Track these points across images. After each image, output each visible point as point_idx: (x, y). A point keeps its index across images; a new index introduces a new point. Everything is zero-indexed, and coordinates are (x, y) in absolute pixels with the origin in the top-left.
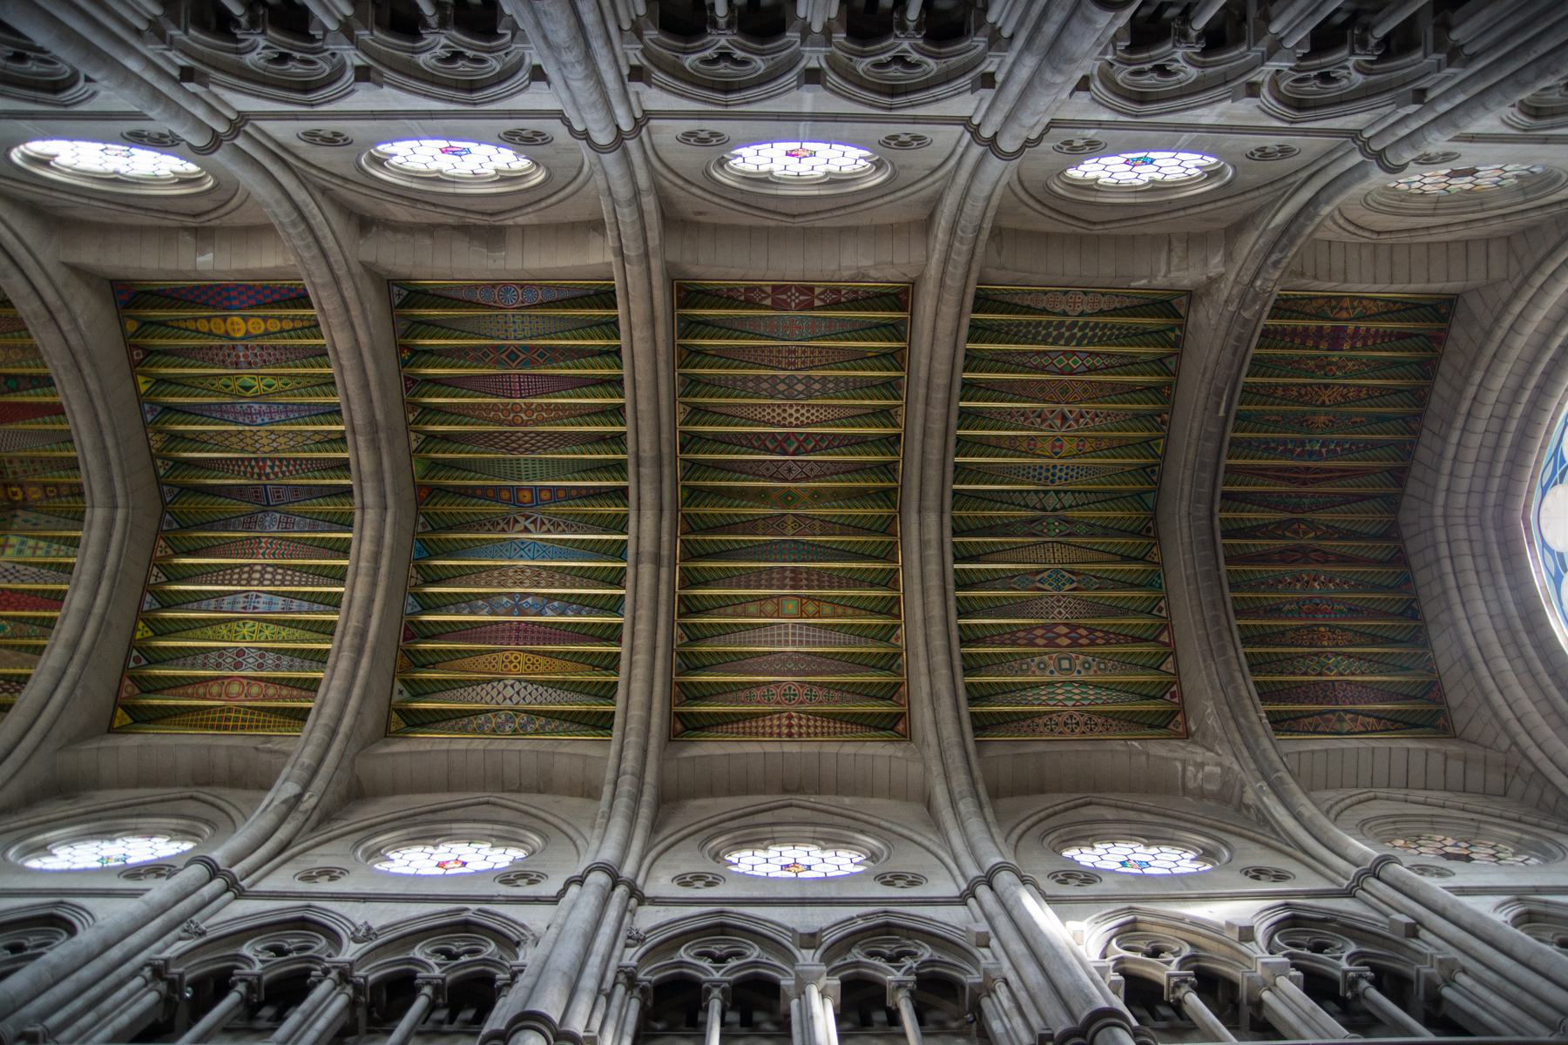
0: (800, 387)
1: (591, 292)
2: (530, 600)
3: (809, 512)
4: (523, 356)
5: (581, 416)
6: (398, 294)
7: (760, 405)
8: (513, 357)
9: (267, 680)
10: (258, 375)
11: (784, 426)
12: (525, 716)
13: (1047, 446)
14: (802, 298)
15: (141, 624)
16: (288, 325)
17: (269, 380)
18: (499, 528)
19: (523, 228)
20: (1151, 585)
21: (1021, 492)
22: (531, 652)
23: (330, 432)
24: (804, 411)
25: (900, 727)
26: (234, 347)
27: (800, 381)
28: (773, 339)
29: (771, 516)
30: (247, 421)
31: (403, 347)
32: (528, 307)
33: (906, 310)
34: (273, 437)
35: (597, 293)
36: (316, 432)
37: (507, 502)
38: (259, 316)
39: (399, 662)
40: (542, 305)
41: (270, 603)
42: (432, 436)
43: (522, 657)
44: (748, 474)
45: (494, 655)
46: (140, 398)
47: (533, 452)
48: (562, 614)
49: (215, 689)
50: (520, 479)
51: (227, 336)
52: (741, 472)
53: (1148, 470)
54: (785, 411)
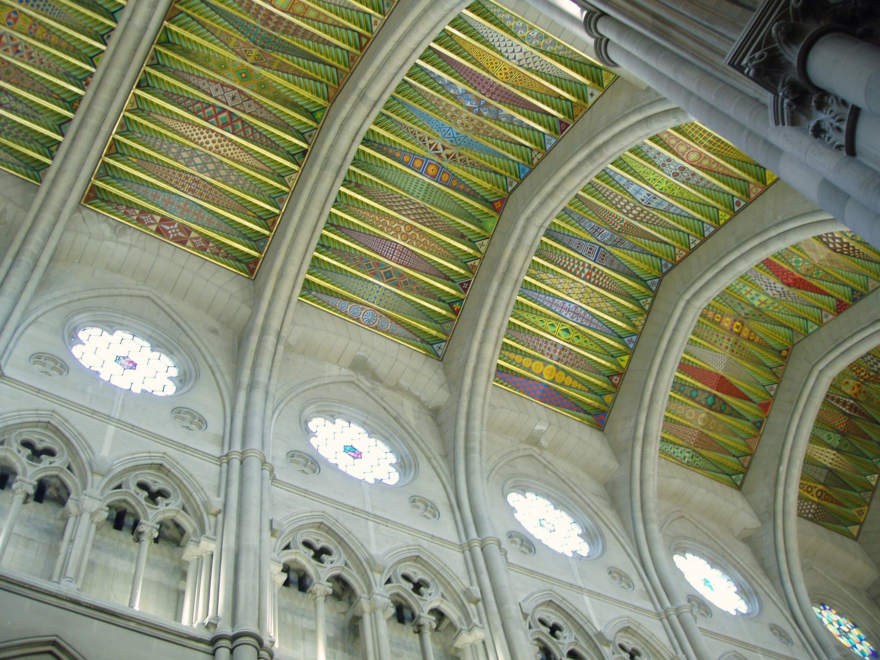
0: (198, 160)
2: (468, 104)
3: (233, 57)
4: (382, 272)
6: (440, 348)
7: (233, 160)
8: (388, 274)
9: (670, 150)
11: (222, 135)
12: (520, 33)
13: (20, 22)
14: (167, 228)
15: (722, 222)
16: (518, 358)
17: (551, 329)
22: (488, 72)
24: (203, 140)
26: (558, 360)
27: (196, 165)
28: (201, 206)
29: (264, 67)
30: (579, 309)
31: (456, 313)
32: (361, 304)
33: (93, 185)
34: (570, 291)
37: (446, 171)
38: (532, 373)
39: (580, 114)
40: (351, 301)
41: (637, 192)
42: (471, 243)
44: (266, 109)
46: (631, 353)
47: (410, 200)
49: (705, 162)
50: (429, 184)
52: (270, 112)
54: (217, 147)
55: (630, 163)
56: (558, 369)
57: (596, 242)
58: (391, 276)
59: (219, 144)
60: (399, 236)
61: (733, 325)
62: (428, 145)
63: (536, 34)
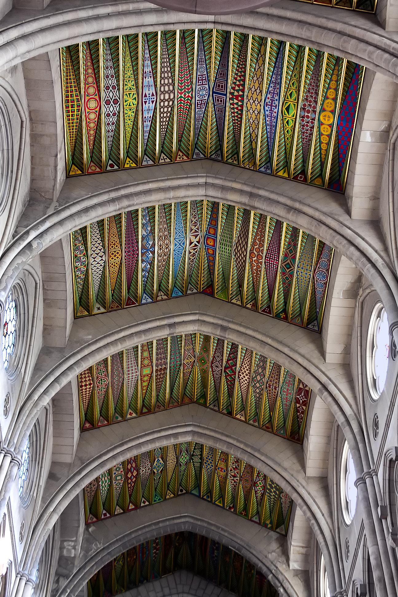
1: (318, 310)
2: (151, 255)
5: (253, 283)
8: (288, 266)
10: (296, 119)
11: (239, 372)
12: (84, 269)
16: (324, 147)
17: (291, 124)
18: (193, 227)
19: (354, 308)
22: (121, 263)
23: (256, 143)
25: (87, 425)
26: (315, 112)
30: (267, 101)
34: (256, 112)
36: (257, 136)
40: (314, 289)
43: (119, 260)
45: (119, 245)
48: (143, 270)
49: (91, 90)
51: (323, 110)
53: (209, 494)
55: (130, 132)
56: (323, 110)
57: (211, 98)
58: (288, 263)
59: (245, 374)
60: (260, 261)
62: (195, 251)
63: (77, 264)
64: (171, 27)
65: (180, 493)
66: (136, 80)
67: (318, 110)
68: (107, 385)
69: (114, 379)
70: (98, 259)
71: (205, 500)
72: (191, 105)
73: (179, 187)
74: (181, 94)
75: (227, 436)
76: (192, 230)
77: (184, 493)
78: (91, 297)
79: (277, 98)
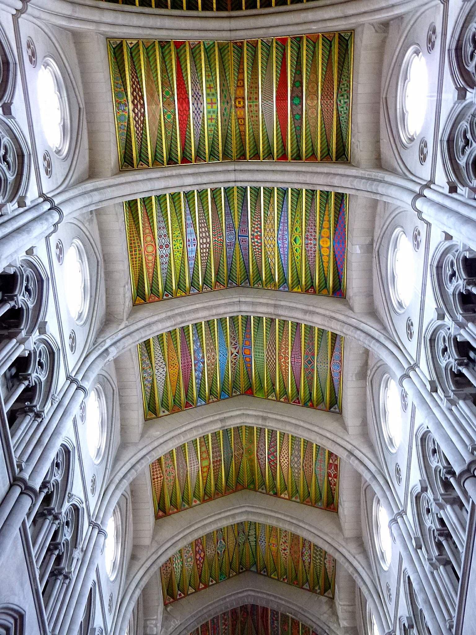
2: (202, 365)
3: (244, 457)
4: (309, 366)
5: (283, 381)
11: (280, 457)
12: (150, 379)
13: (274, 542)
16: (325, 265)
17: (299, 251)
20: (221, 575)
21: (255, 528)
22: (179, 373)
23: (275, 270)
25: (161, 513)
26: (315, 239)
28: (316, 461)
30: (279, 236)
34: (272, 246)
35: (336, 398)
36: (274, 264)
38: (330, 254)
45: (176, 359)
48: (196, 378)
49: (149, 239)
53: (265, 570)
56: (321, 237)
61: (240, 108)
64: (204, 187)
65: (241, 571)
66: (181, 229)
67: (317, 237)
68: (174, 477)
69: (180, 471)
70: (161, 370)
71: (262, 574)
72: (223, 246)
73: (219, 306)
74: (215, 238)
75: (275, 512)
76: (232, 343)
77: (245, 571)
78: (157, 402)
79: (286, 233)
